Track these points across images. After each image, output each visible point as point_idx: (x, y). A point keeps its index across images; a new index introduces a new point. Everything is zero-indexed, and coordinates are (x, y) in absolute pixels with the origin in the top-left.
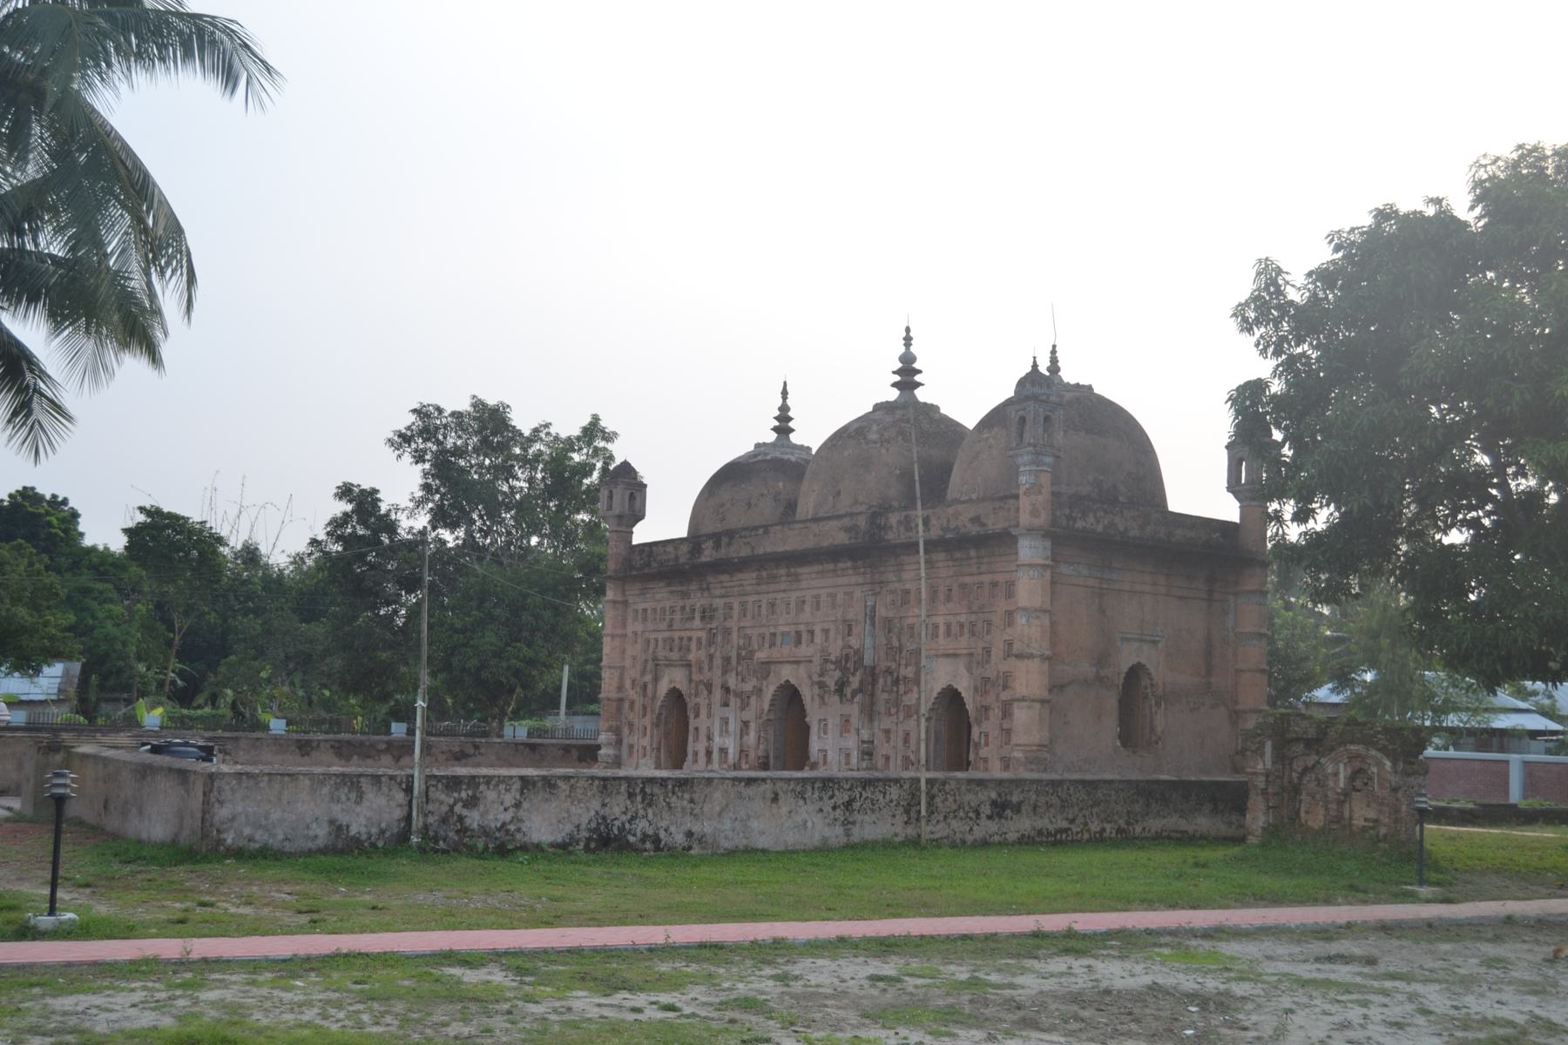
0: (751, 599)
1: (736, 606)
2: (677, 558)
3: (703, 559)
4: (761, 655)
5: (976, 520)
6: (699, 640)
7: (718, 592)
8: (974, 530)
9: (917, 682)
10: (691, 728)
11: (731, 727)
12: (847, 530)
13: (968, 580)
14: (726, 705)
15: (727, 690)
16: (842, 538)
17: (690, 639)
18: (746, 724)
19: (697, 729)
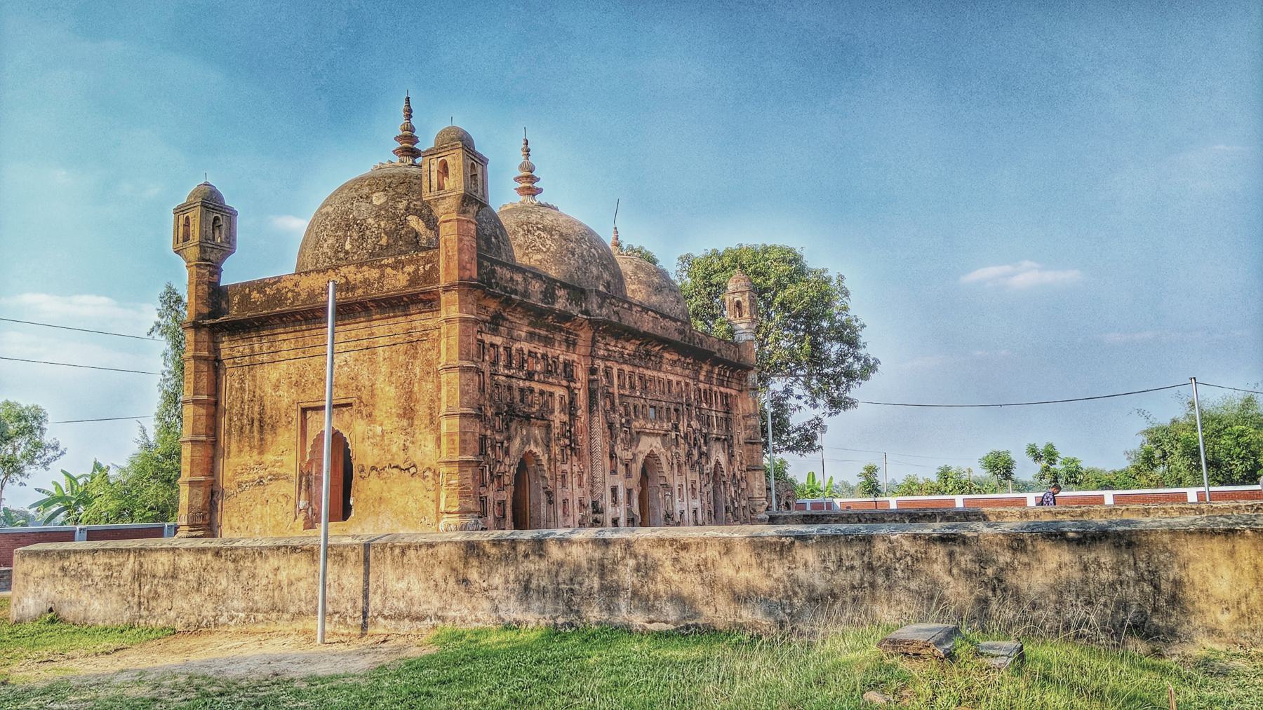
0: (627, 368)
1: (615, 372)
2: (526, 294)
3: (557, 306)
4: (637, 424)
5: (719, 350)
6: (562, 397)
7: (601, 352)
8: (718, 355)
9: (708, 456)
10: (560, 501)
11: (621, 494)
12: (681, 332)
13: (722, 389)
14: (614, 472)
15: (612, 456)
16: (676, 337)
17: (551, 394)
18: (629, 492)
19: (565, 501)
